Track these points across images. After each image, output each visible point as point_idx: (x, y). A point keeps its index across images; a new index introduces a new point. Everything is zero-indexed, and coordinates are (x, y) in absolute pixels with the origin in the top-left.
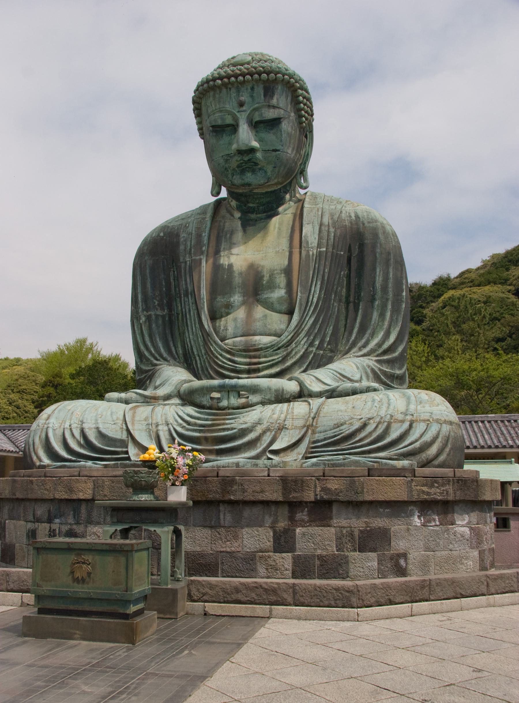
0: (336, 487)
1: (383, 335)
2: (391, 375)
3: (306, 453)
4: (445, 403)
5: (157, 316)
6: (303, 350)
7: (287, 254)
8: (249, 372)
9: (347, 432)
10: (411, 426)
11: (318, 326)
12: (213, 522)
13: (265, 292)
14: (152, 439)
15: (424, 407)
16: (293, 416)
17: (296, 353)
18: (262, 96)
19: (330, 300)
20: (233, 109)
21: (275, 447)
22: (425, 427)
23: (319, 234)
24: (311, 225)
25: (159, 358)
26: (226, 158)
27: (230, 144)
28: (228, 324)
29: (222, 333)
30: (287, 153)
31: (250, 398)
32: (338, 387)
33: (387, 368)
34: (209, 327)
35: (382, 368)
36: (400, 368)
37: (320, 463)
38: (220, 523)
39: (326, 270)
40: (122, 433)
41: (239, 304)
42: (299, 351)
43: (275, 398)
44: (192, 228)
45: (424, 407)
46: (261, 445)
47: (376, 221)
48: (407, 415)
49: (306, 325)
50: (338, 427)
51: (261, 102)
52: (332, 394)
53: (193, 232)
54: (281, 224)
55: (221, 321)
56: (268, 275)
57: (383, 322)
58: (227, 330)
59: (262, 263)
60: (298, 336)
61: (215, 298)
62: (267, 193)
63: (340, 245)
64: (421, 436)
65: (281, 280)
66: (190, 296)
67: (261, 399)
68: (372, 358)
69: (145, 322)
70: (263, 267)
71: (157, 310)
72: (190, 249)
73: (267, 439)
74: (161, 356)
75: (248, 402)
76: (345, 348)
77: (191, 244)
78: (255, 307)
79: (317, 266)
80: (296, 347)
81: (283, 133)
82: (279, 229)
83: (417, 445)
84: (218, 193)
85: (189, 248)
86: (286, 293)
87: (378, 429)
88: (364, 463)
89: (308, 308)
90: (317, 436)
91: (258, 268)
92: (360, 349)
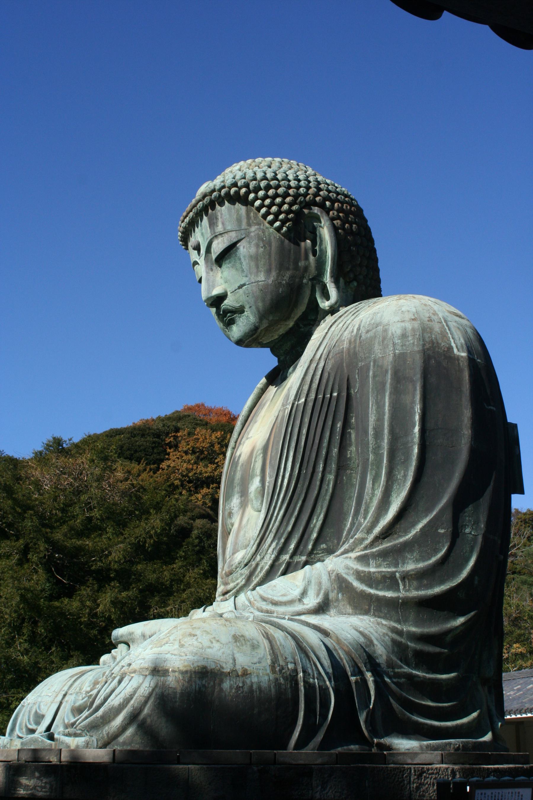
17: (262, 569)
18: (208, 228)
30: (259, 281)
42: (266, 563)
80: (263, 558)
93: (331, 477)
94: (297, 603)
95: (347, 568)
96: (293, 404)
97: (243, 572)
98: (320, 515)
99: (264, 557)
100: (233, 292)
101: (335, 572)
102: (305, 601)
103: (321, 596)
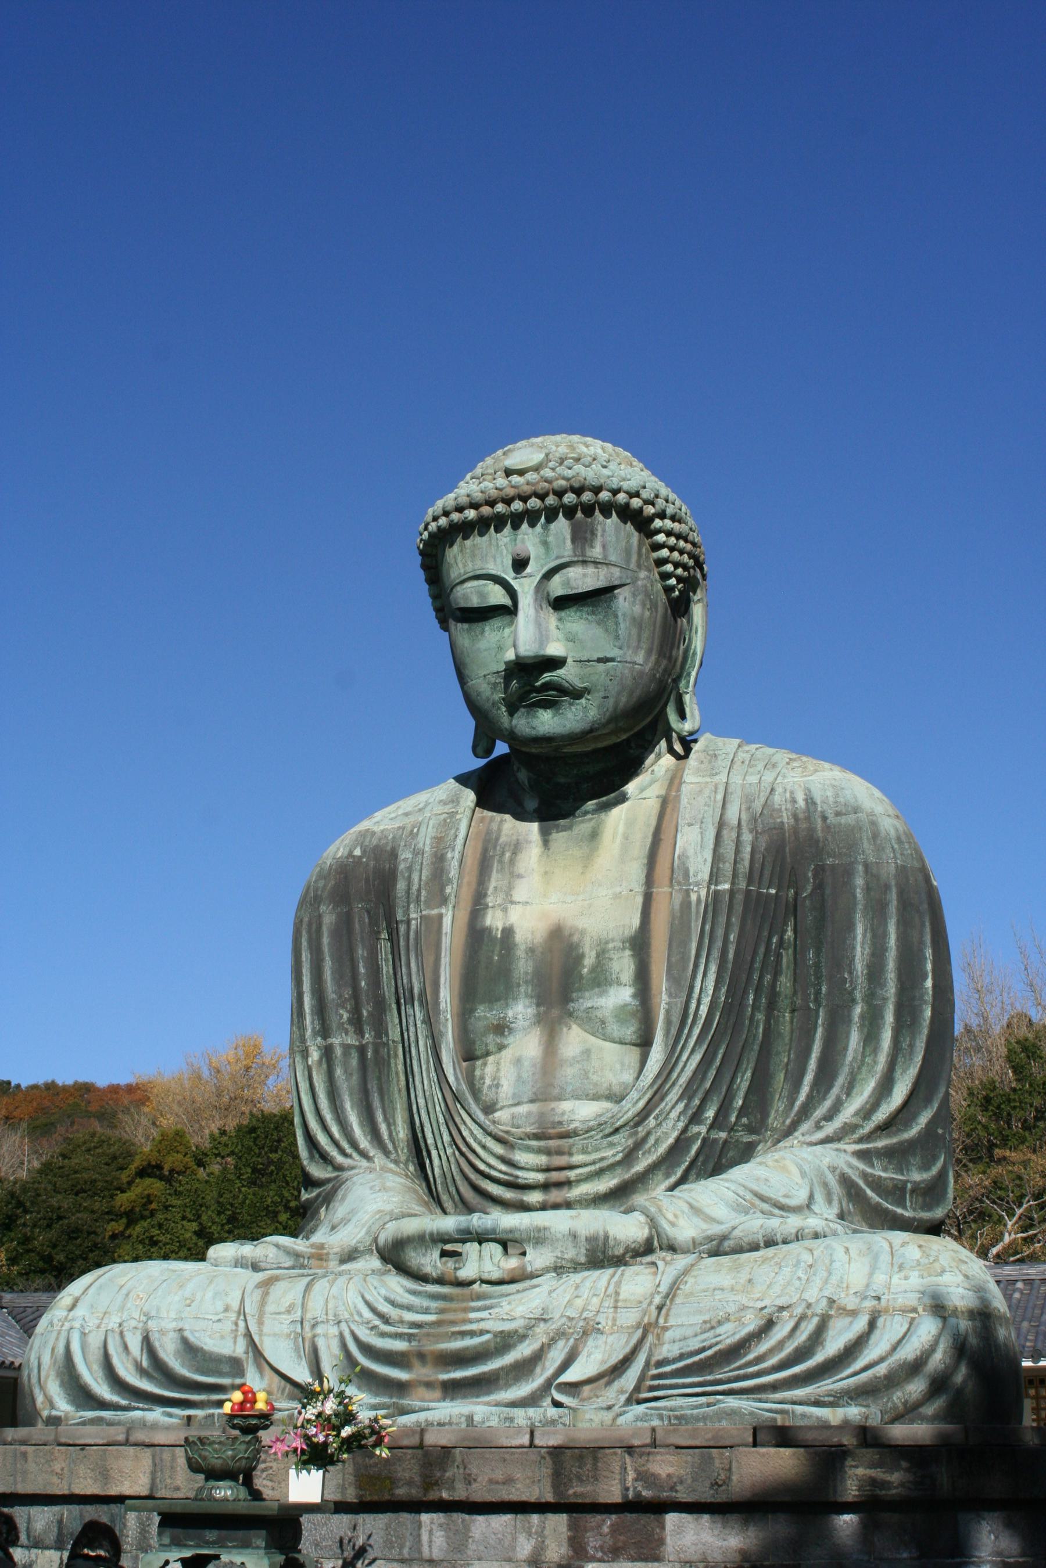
0: (671, 1470)
1: (874, 1089)
2: (895, 1186)
3: (637, 1389)
4: (963, 1267)
5: (347, 1048)
6: (675, 1134)
7: (639, 900)
8: (545, 1187)
9: (729, 1341)
10: (872, 1325)
11: (712, 1073)
12: (406, 1551)
13: (587, 994)
14: (300, 1356)
15: (906, 1278)
16: (616, 1301)
18: (569, 542)
19: (742, 1005)
20: (504, 571)
21: (571, 1375)
22: (906, 1326)
23: (715, 850)
24: (696, 829)
25: (349, 1150)
26: (493, 680)
27: (500, 648)
28: (502, 1074)
29: (487, 1094)
30: (635, 663)
31: (528, 1257)
32: (734, 1228)
33: (885, 1170)
34: (457, 1078)
35: (869, 1170)
36: (925, 1167)
37: (651, 1415)
38: (420, 1552)
39: (732, 937)
40: (235, 1342)
41: (527, 1023)
43: (587, 1256)
44: (425, 840)
45: (906, 1278)
46: (543, 1369)
47: (856, 810)
48: (865, 1298)
49: (682, 1070)
50: (713, 1328)
51: (566, 554)
52: (719, 1247)
53: (427, 849)
54: (630, 823)
55: (485, 1064)
56: (593, 954)
57: (876, 1055)
58: (498, 1086)
59: (582, 923)
60: (662, 1099)
61: (472, 1010)
62: (595, 751)
63: (767, 873)
64: (894, 1348)
65: (624, 966)
66: (416, 1003)
67: (553, 1259)
68: (846, 1147)
69: (320, 1061)
70: (583, 932)
71: (347, 1034)
72: (419, 891)
73: (556, 1356)
74: (354, 1145)
75: (523, 1268)
76: (784, 1122)
77: (420, 879)
78: (565, 1029)
79: (708, 927)
80: (659, 1125)
81: (621, 619)
82: (626, 837)
83: (881, 1370)
84: (489, 751)
85: (415, 887)
86: (634, 996)
87: (798, 1333)
88: (751, 1413)
89: (686, 1031)
90: (668, 1350)
91: (571, 935)
92: (818, 1127)
93: (760, 1016)
94: (806, 1211)
95: (850, 1166)
96: (709, 888)
97: (616, 1141)
98: (745, 1072)
99: (660, 1124)
100: (581, 661)
101: (838, 1171)
102: (815, 1208)
103: (835, 1203)
